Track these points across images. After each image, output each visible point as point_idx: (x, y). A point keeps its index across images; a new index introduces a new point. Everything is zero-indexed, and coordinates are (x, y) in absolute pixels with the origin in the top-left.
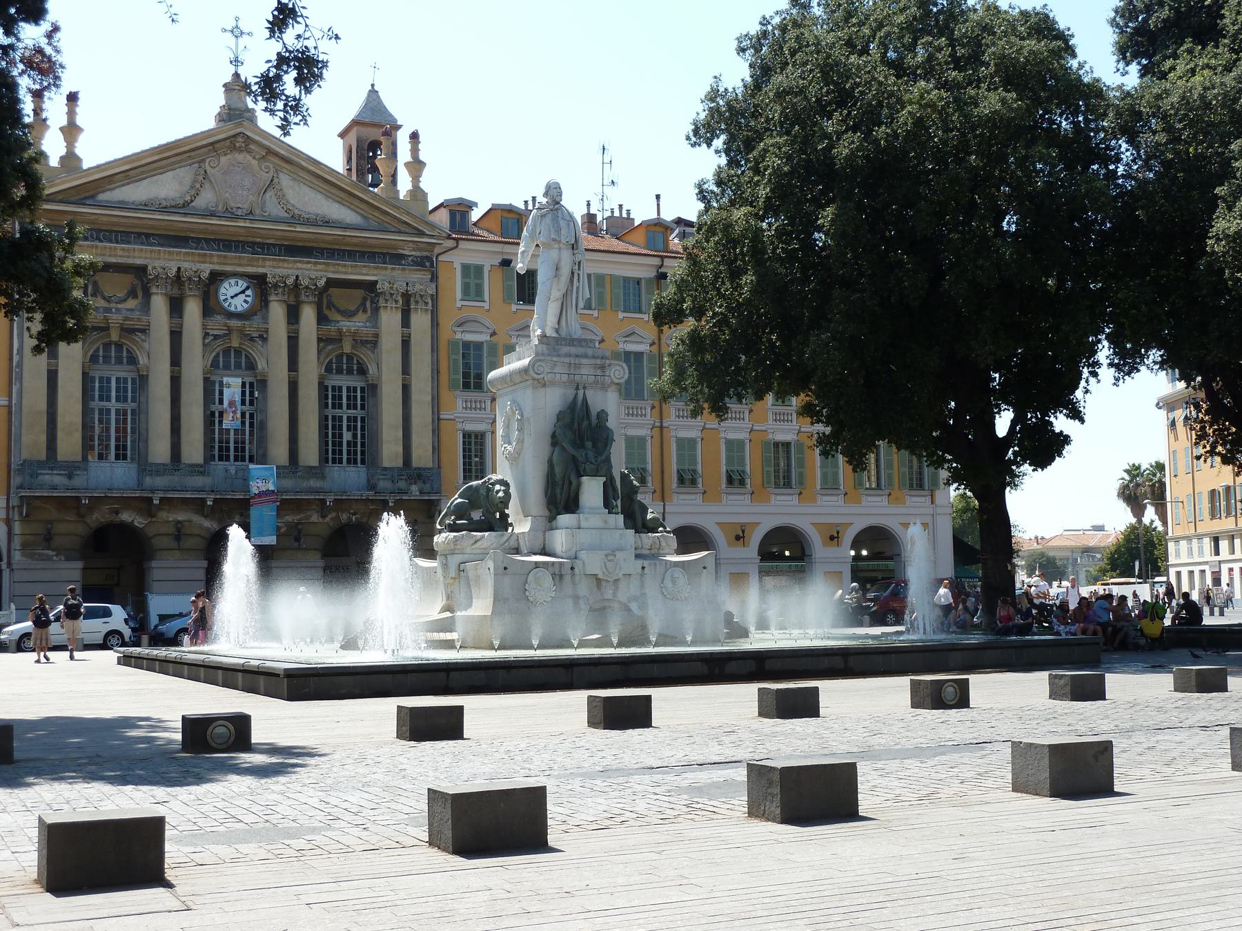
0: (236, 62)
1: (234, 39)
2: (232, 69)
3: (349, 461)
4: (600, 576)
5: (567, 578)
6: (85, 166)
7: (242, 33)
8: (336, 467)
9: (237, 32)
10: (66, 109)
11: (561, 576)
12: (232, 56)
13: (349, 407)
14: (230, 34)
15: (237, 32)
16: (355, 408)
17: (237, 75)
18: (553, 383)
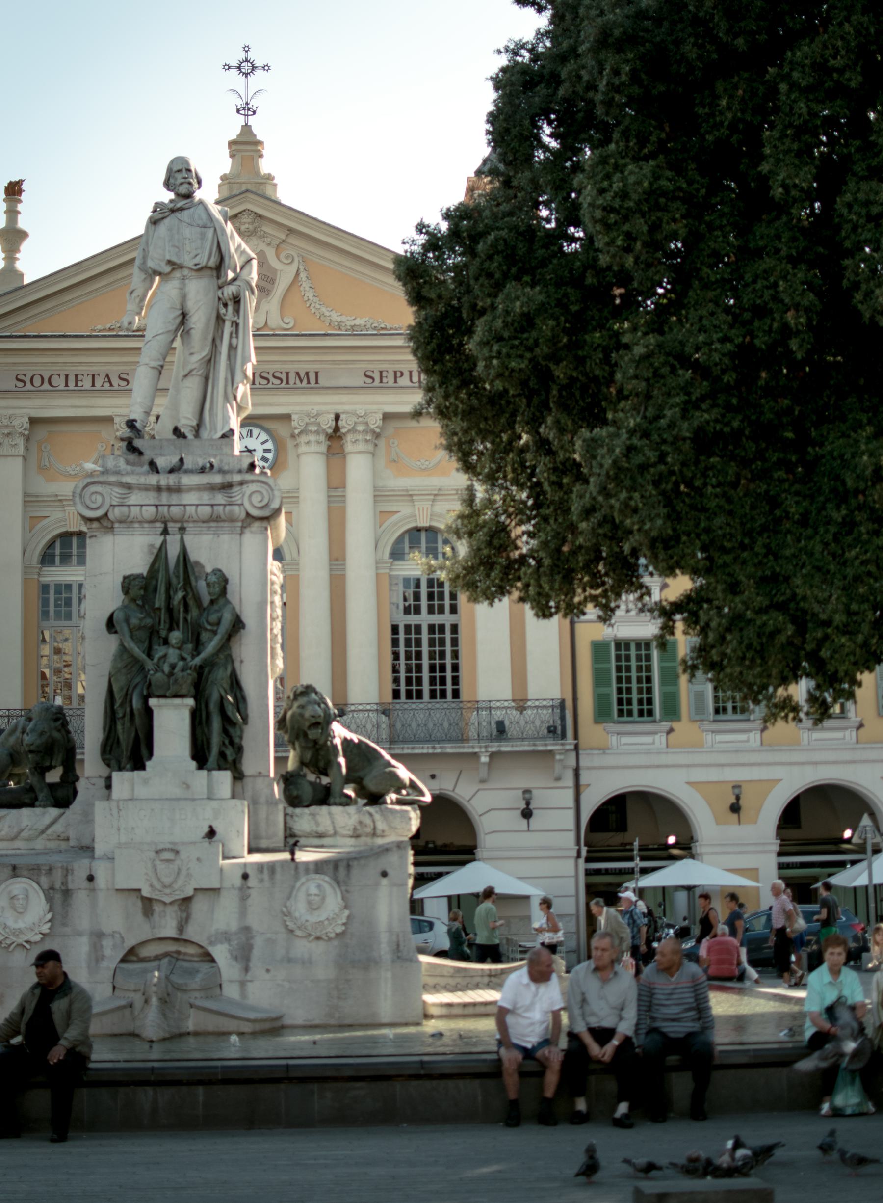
0: (246, 110)
1: (242, 78)
2: (240, 120)
3: (433, 695)
4: (146, 893)
5: (81, 898)
6: (27, 280)
7: (254, 68)
8: (414, 704)
9: (246, 67)
10: (4, 206)
11: (67, 893)
12: (240, 103)
13: (431, 611)
14: (235, 72)
15: (246, 67)
16: (441, 611)
17: (246, 128)
18: (127, 522)
